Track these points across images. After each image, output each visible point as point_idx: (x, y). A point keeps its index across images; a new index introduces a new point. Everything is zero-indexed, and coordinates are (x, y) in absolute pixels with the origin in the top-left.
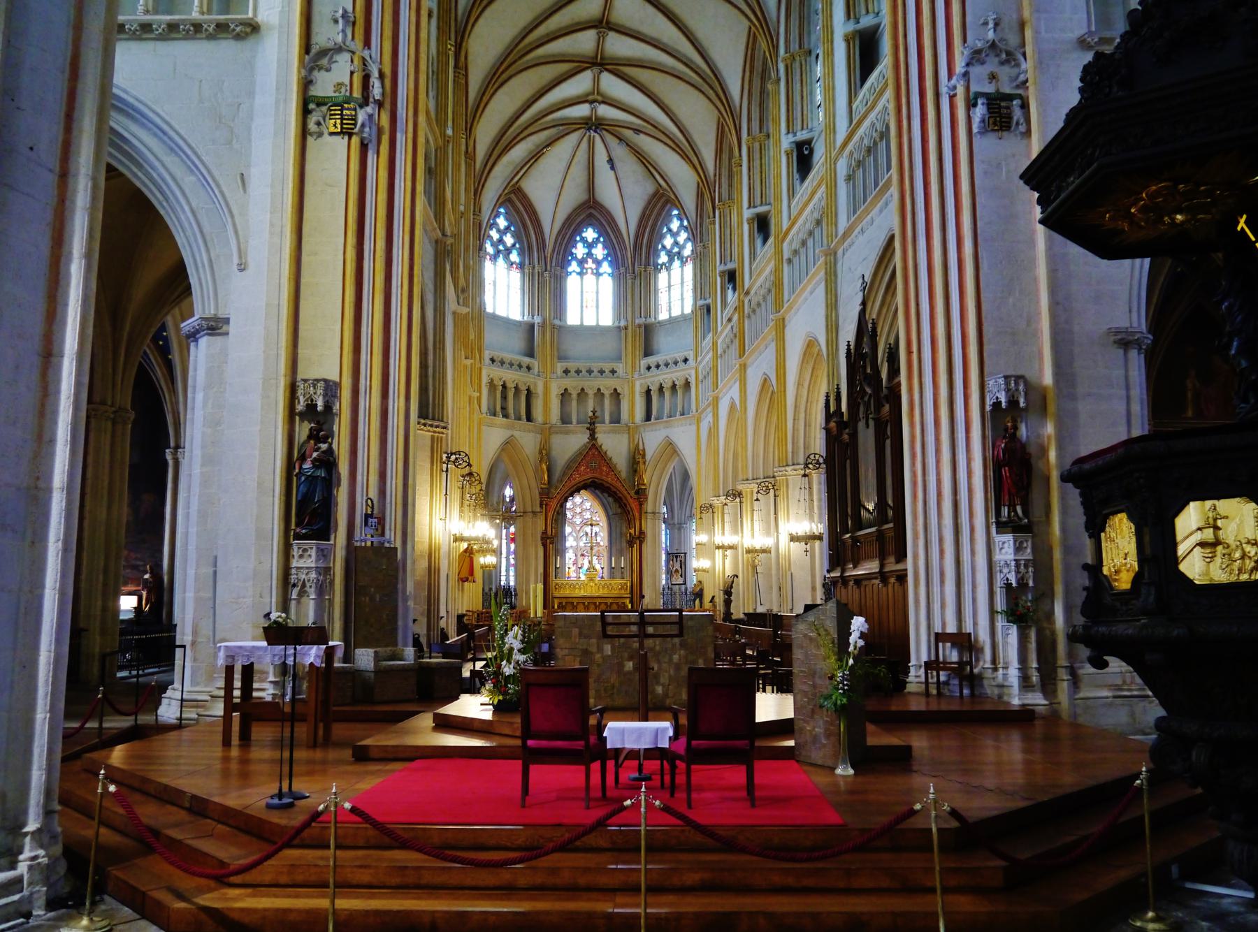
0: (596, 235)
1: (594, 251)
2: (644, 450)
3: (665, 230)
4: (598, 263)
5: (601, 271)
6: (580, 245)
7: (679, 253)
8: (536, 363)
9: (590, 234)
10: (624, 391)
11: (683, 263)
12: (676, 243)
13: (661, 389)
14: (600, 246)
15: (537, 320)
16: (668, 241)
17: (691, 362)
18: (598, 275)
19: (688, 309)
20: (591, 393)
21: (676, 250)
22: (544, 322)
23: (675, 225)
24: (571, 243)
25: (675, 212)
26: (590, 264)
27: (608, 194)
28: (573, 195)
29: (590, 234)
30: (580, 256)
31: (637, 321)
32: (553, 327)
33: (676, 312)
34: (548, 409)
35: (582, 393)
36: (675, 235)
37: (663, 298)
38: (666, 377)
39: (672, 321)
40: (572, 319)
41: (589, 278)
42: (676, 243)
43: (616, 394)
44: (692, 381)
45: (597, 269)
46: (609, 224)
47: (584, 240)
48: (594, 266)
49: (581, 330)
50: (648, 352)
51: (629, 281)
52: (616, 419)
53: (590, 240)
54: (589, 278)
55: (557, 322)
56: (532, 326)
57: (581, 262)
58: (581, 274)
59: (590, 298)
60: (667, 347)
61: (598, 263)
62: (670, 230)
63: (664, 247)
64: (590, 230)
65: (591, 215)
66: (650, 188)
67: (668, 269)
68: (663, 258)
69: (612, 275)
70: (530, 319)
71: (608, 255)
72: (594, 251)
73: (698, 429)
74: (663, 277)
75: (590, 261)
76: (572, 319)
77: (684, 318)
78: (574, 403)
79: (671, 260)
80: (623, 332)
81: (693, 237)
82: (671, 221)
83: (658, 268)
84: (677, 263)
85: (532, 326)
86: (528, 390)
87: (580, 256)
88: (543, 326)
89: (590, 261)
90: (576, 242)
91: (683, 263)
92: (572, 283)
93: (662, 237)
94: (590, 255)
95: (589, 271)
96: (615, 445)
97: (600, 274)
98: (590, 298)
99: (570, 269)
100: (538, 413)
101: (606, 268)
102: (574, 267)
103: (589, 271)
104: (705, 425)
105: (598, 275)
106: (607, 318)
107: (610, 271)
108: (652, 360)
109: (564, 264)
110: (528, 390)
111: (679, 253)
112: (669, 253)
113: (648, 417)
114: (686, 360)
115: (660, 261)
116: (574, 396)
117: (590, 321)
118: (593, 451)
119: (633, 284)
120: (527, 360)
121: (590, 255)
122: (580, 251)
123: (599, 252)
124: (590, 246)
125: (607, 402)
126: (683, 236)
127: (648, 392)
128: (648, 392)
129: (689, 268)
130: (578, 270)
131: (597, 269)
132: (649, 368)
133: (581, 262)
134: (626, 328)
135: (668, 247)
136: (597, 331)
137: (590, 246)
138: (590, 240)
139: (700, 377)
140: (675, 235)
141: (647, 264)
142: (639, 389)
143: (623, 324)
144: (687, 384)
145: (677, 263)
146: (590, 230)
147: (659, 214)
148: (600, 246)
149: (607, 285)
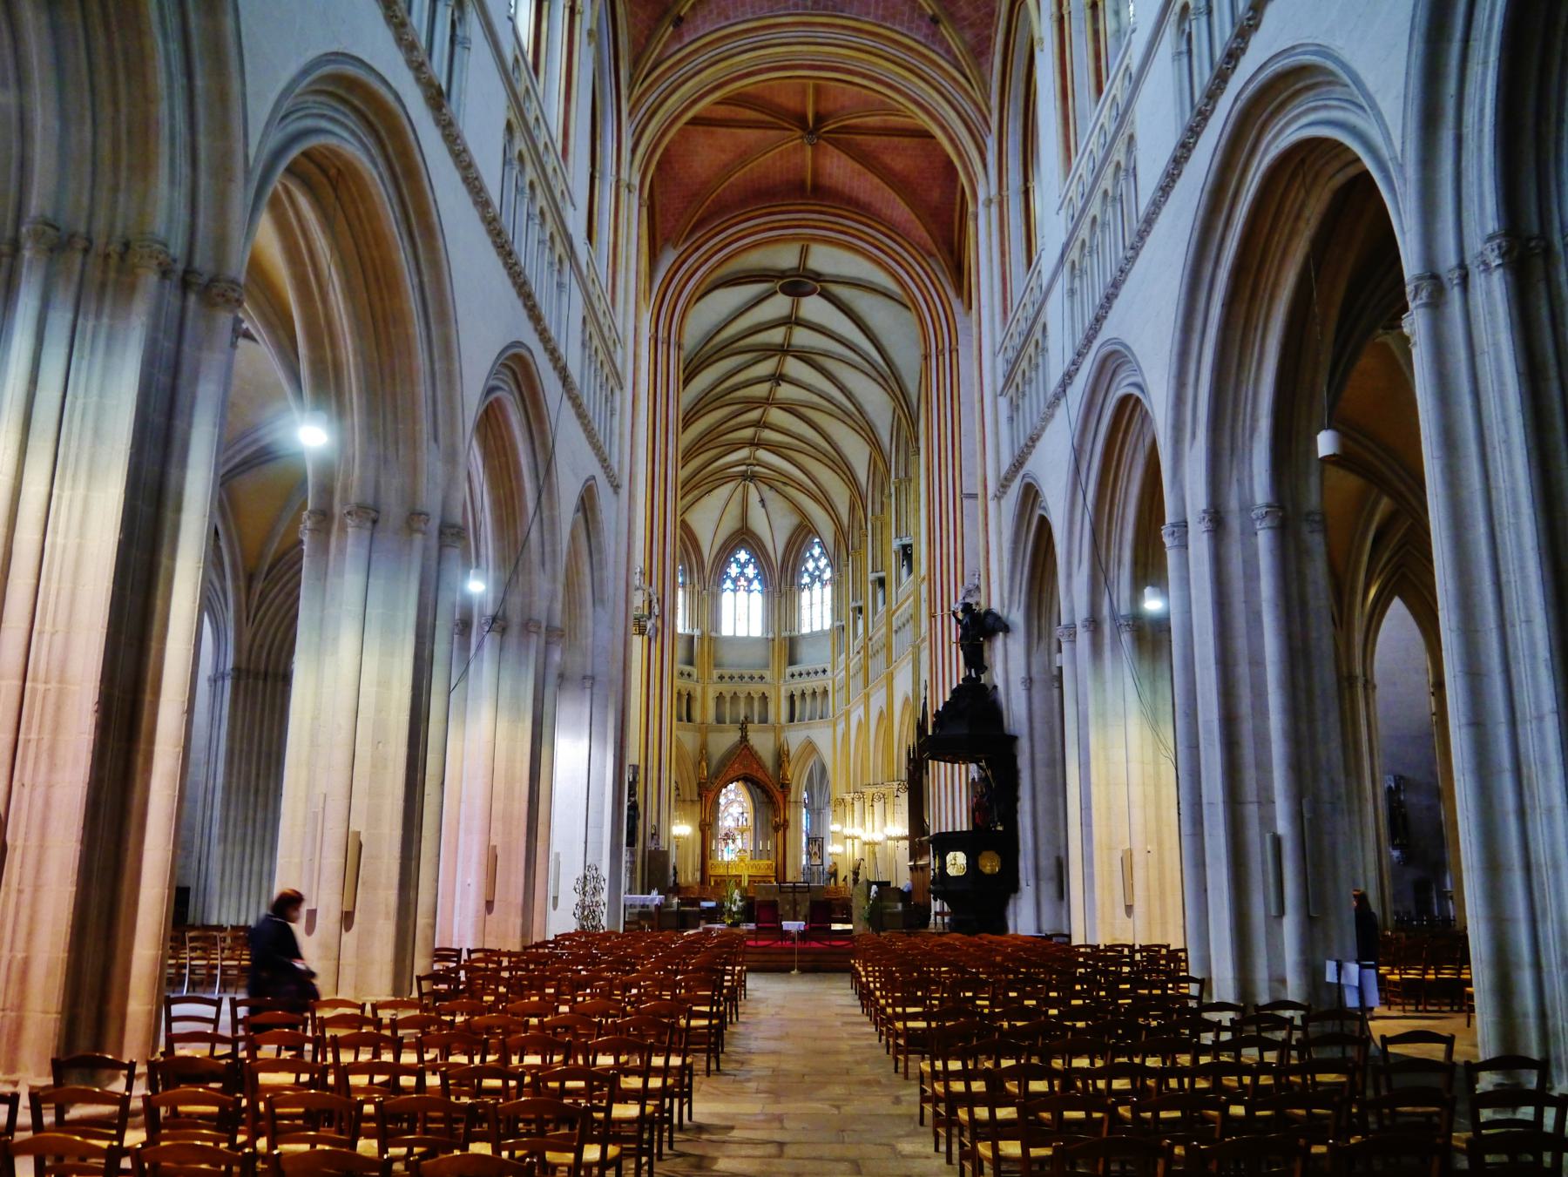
0: (748, 557)
1: (746, 571)
2: (788, 750)
3: (808, 555)
4: (750, 582)
5: (752, 588)
6: (734, 565)
7: (819, 576)
8: (695, 670)
9: (743, 556)
10: (771, 694)
11: (823, 586)
12: (817, 568)
13: (803, 694)
14: (751, 566)
15: (697, 632)
16: (810, 565)
17: (829, 673)
18: (750, 591)
19: (827, 626)
20: (742, 696)
21: (817, 573)
22: (703, 634)
23: (817, 551)
24: (727, 564)
25: (817, 540)
26: (743, 582)
27: (758, 522)
28: (730, 524)
29: (743, 556)
30: (733, 575)
31: (784, 634)
32: (710, 638)
33: (817, 628)
34: (706, 710)
35: (735, 697)
36: (816, 560)
37: (805, 614)
38: (808, 684)
39: (813, 635)
40: (726, 630)
41: (742, 594)
42: (817, 568)
43: (764, 698)
44: (830, 689)
45: (749, 586)
46: (760, 549)
47: (738, 561)
48: (745, 584)
49: (734, 640)
51: (776, 599)
52: (764, 720)
53: (742, 561)
54: (742, 594)
55: (713, 634)
56: (692, 637)
57: (735, 581)
58: (735, 591)
59: (742, 610)
60: (810, 657)
61: (750, 582)
62: (812, 555)
63: (807, 570)
64: (743, 552)
65: (743, 540)
66: (794, 520)
67: (810, 589)
68: (806, 579)
69: (761, 592)
70: (690, 632)
71: (758, 574)
72: (746, 571)
73: (834, 730)
74: (805, 595)
75: (742, 579)
76: (726, 630)
78: (728, 705)
79: (813, 582)
80: (771, 644)
81: (831, 564)
82: (813, 548)
83: (801, 588)
84: (817, 585)
85: (692, 637)
86: (689, 694)
87: (733, 575)
88: (702, 638)
89: (742, 579)
90: (730, 563)
91: (823, 586)
92: (727, 599)
93: (806, 561)
94: (742, 574)
95: (742, 588)
96: (762, 743)
97: (751, 591)
98: (742, 610)
99: (725, 587)
100: (697, 714)
101: (756, 585)
102: (728, 584)
103: (742, 588)
104: (841, 728)
105: (750, 591)
106: (757, 630)
107: (759, 588)
108: (795, 669)
109: (720, 582)
110: (689, 694)
111: (819, 576)
112: (811, 575)
113: (792, 719)
114: (824, 671)
115: (803, 582)
116: (728, 698)
117: (741, 633)
118: (744, 748)
119: (780, 603)
120: (687, 668)
121: (742, 574)
122: (734, 570)
123: (750, 571)
124: (743, 566)
125: (756, 705)
126: (823, 562)
127: (792, 696)
128: (792, 696)
129: (828, 590)
130: (732, 587)
131: (749, 586)
132: (793, 676)
133: (735, 581)
134: (773, 640)
135: (811, 570)
136: (748, 641)
138: (742, 561)
139: (837, 688)
140: (816, 560)
141: (792, 584)
142: (784, 694)
143: (770, 636)
144: (825, 692)
145: (817, 585)
146: (743, 552)
147: (803, 542)
148: (751, 566)
149: (757, 600)
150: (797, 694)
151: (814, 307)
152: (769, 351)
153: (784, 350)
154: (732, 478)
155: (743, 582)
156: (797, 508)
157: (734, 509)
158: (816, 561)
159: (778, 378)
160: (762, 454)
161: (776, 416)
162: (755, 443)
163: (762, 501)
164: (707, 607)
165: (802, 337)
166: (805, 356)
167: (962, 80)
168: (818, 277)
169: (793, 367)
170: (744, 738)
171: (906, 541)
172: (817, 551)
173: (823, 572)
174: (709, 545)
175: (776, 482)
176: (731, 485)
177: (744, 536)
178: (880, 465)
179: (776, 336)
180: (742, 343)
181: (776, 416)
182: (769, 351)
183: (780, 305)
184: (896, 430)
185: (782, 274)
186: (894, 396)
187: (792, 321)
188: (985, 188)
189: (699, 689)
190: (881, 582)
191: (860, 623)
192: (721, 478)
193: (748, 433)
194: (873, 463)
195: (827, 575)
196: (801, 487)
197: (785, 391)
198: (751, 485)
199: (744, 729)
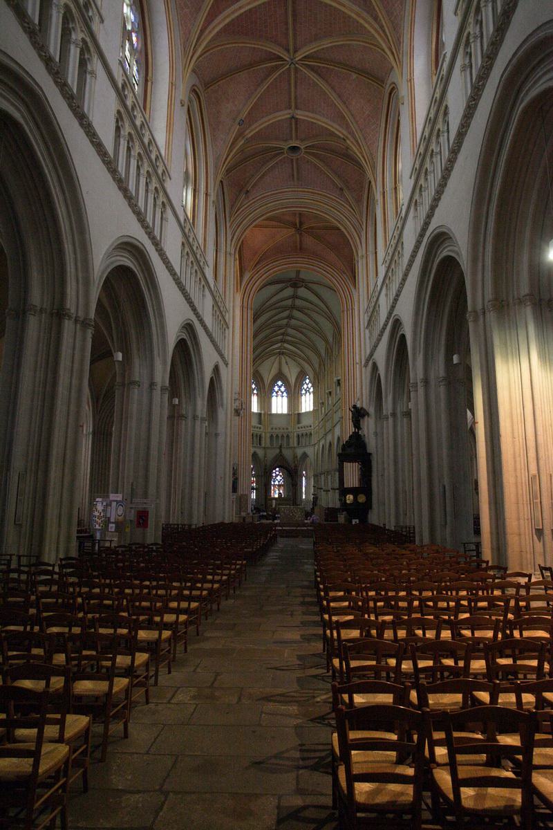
4: (283, 393)
9: (280, 383)
10: (291, 435)
13: (302, 435)
15: (262, 412)
16: (305, 386)
17: (312, 428)
19: (312, 409)
26: (280, 393)
27: (285, 370)
28: (274, 371)
29: (280, 383)
30: (276, 390)
33: (308, 410)
34: (266, 442)
36: (307, 384)
38: (304, 431)
40: (274, 411)
41: (279, 397)
43: (288, 436)
47: (278, 385)
49: (277, 415)
50: (299, 422)
52: (288, 443)
54: (279, 397)
57: (277, 392)
58: (277, 396)
60: (305, 422)
61: (283, 393)
68: (304, 392)
69: (287, 397)
76: (274, 411)
77: (310, 412)
84: (308, 394)
85: (260, 414)
87: (276, 390)
88: (264, 414)
92: (274, 399)
94: (280, 390)
96: (287, 453)
100: (263, 442)
101: (285, 394)
105: (282, 396)
106: (285, 411)
108: (300, 425)
112: (305, 390)
113: (299, 444)
114: (311, 426)
117: (280, 412)
121: (280, 390)
122: (276, 388)
124: (280, 387)
125: (285, 439)
126: (310, 385)
127: (299, 436)
128: (299, 436)
129: (312, 395)
133: (277, 392)
136: (282, 415)
137: (280, 387)
140: (307, 384)
144: (311, 434)
145: (308, 394)
149: (285, 400)
150: (300, 435)
151: (302, 292)
152: (285, 308)
153: (293, 307)
154: (275, 354)
155: (280, 393)
157: (276, 365)
158: (308, 384)
159: (290, 317)
160: (286, 345)
161: (290, 331)
162: (282, 341)
163: (286, 362)
164: (265, 401)
165: (298, 302)
166: (300, 310)
167: (350, 209)
168: (303, 281)
169: (296, 314)
170: (281, 451)
171: (338, 378)
172: (307, 381)
173: (310, 389)
174: (267, 379)
175: (292, 355)
176: (273, 358)
178: (330, 351)
179: (289, 302)
180: (279, 304)
181: (290, 331)
182: (285, 308)
183: (289, 292)
184: (334, 336)
185: (290, 280)
186: (333, 324)
187: (295, 297)
188: (361, 252)
189: (263, 434)
190: (330, 393)
191: (323, 408)
192: (271, 354)
194: (327, 349)
195: (312, 390)
196: (300, 357)
197: (293, 322)
198: (283, 357)
199: (281, 447)
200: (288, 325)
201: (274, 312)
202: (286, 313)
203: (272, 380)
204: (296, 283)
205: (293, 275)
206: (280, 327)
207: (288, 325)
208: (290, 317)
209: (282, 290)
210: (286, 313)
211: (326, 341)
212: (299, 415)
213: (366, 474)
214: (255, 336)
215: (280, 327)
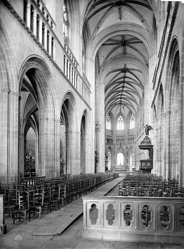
28: (118, 112)
29: (120, 117)
40: (118, 129)
41: (120, 123)
54: (120, 123)
76: (118, 129)
92: (118, 124)
101: (123, 122)
122: (119, 119)
123: (122, 119)
151: (128, 74)
152: (121, 83)
153: (124, 82)
156: (128, 107)
158: (133, 117)
161: (124, 93)
165: (126, 80)
168: (128, 69)
176: (117, 106)
177: (120, 114)
179: (122, 80)
180: (119, 81)
181: (124, 93)
182: (121, 83)
183: (122, 75)
192: (116, 104)
193: (120, 96)
200: (122, 91)
201: (116, 85)
202: (122, 85)
203: (117, 115)
204: (125, 70)
205: (122, 67)
206: (120, 91)
207: (122, 91)
208: (123, 87)
209: (119, 74)
210: (122, 85)
211: (140, 97)
212: (129, 130)
213: (151, 154)
214: (106, 90)
215: (120, 91)
